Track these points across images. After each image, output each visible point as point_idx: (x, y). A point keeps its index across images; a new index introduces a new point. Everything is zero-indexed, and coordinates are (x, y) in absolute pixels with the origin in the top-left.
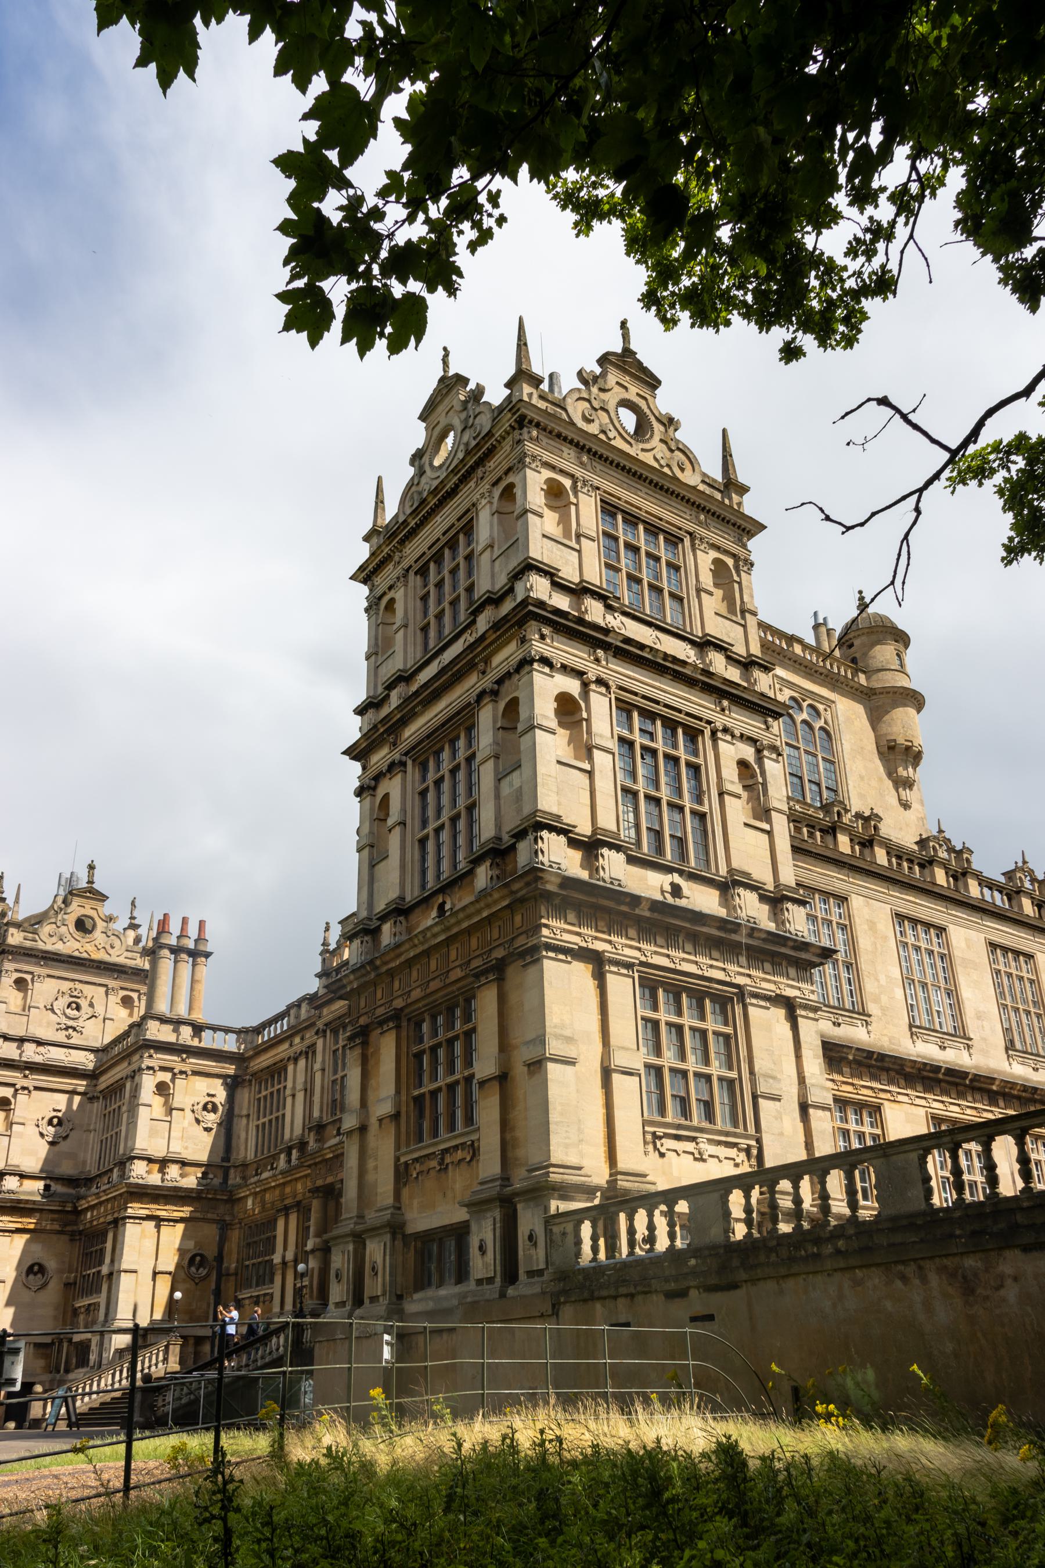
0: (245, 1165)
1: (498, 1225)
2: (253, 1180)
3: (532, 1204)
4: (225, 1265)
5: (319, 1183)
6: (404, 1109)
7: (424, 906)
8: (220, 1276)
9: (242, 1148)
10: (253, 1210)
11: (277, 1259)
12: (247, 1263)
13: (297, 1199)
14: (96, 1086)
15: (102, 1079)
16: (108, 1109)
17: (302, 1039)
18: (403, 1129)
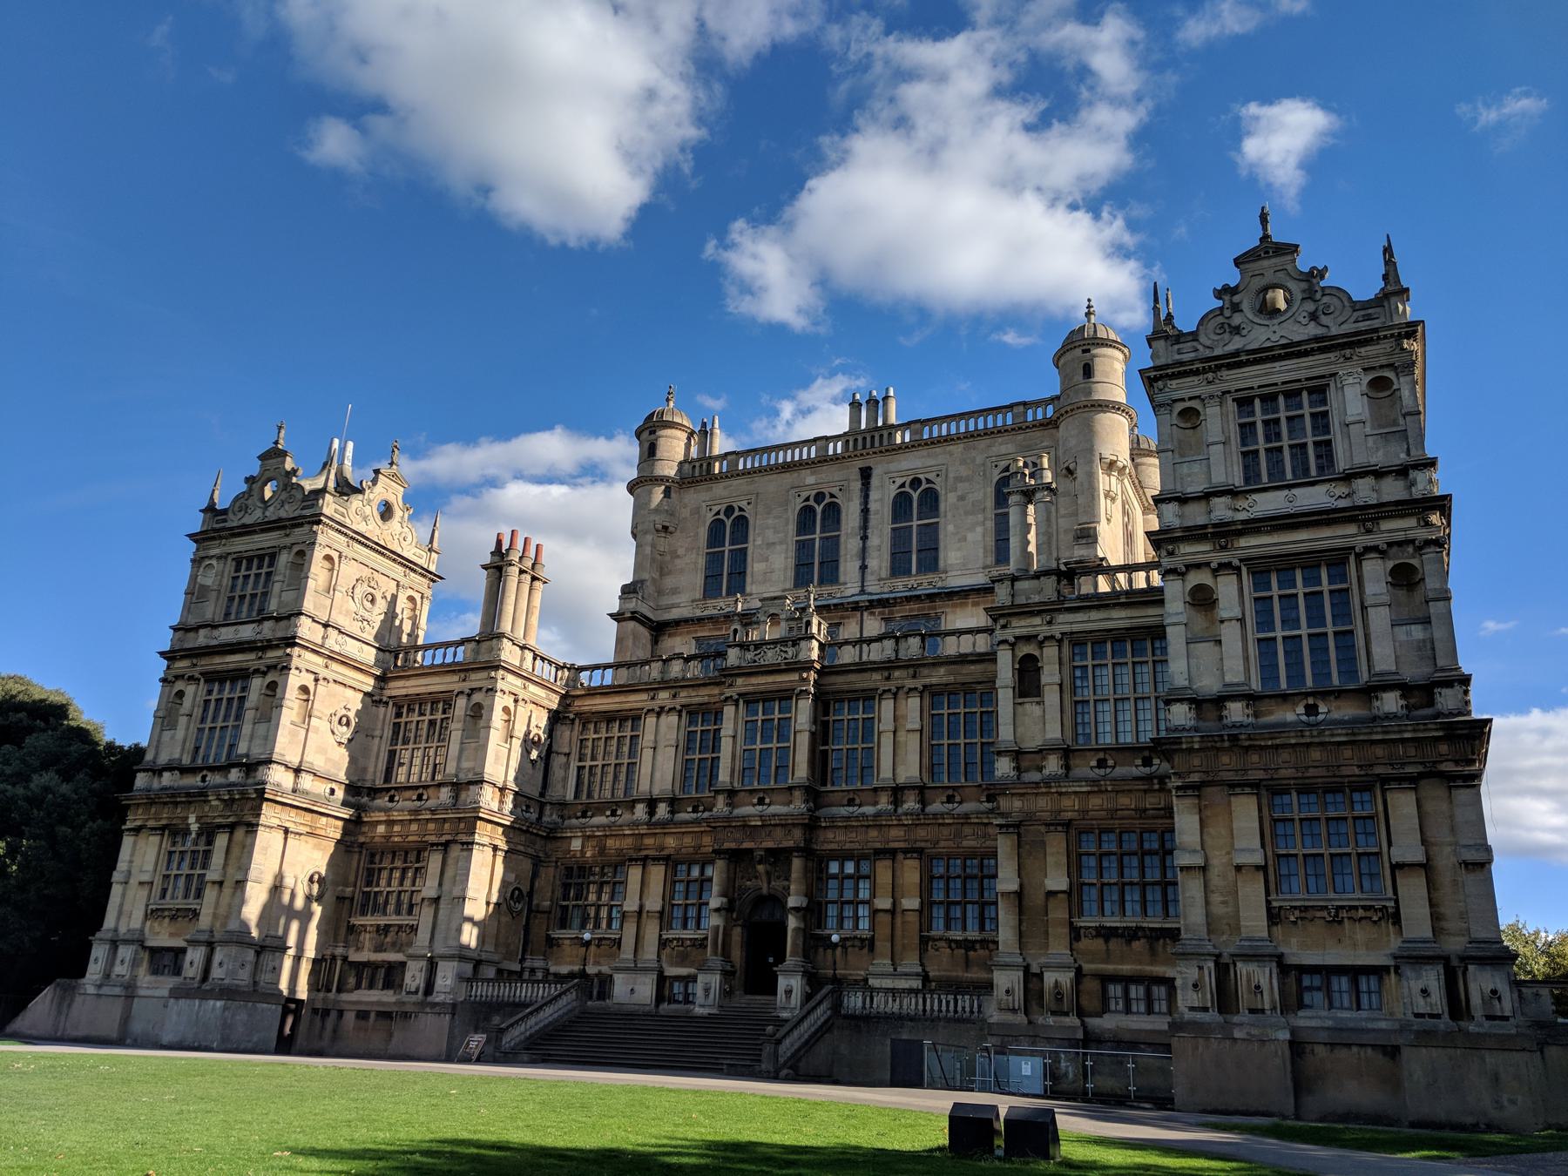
0: (562, 805)
1: (1442, 977)
2: (574, 821)
3: (1488, 968)
4: (535, 902)
5: (727, 845)
6: (1270, 862)
7: (1280, 700)
8: (530, 911)
9: (559, 786)
10: (583, 852)
11: (631, 905)
12: (564, 903)
13: (665, 853)
14: (382, 689)
15: (392, 684)
16: (403, 720)
17: (674, 696)
18: (1272, 878)
